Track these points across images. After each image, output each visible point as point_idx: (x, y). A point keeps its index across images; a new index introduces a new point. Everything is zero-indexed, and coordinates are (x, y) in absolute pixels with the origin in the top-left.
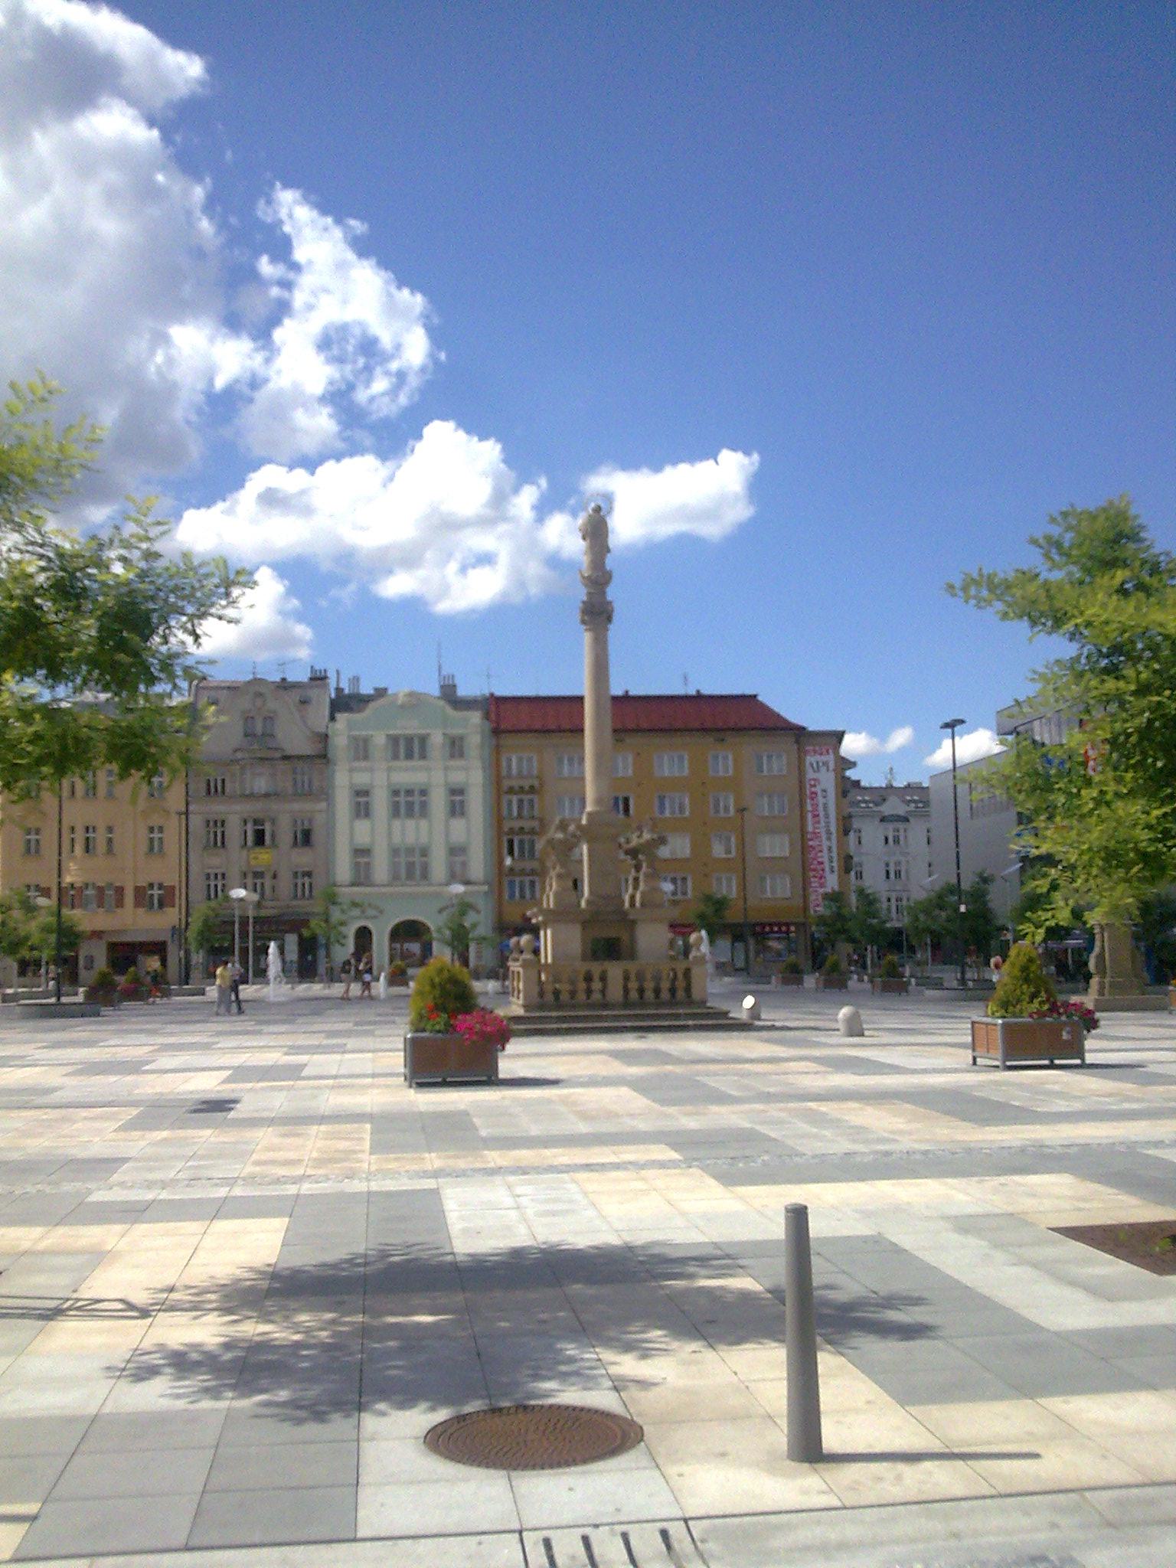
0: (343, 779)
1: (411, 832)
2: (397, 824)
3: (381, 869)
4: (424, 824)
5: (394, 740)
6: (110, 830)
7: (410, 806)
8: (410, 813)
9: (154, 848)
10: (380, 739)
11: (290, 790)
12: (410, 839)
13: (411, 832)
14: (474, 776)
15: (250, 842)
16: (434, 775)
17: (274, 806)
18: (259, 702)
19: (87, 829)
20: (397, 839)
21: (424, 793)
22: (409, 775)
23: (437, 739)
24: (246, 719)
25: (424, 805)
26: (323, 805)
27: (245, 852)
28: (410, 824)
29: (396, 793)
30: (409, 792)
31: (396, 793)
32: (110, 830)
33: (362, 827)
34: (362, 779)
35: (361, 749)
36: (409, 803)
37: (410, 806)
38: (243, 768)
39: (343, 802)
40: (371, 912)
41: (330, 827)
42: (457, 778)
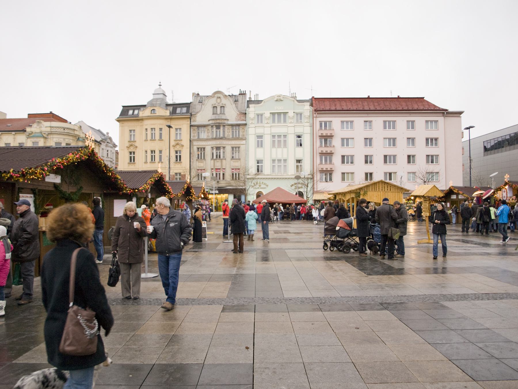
0: (252, 131)
1: (279, 153)
2: (274, 150)
3: (267, 169)
4: (285, 150)
5: (273, 114)
6: (161, 152)
7: (279, 142)
8: (279, 146)
9: (178, 159)
10: (267, 114)
11: (231, 137)
12: (279, 157)
13: (279, 153)
14: (305, 130)
15: (215, 157)
16: (290, 130)
17: (224, 142)
18: (219, 100)
19: (152, 151)
20: (274, 157)
21: (285, 136)
22: (279, 129)
23: (291, 114)
24: (214, 107)
25: (285, 141)
26: (244, 142)
27: (212, 161)
28: (280, 150)
29: (274, 136)
30: (279, 136)
31: (274, 136)
32: (161, 152)
33: (260, 150)
34: (260, 131)
35: (260, 116)
36: (279, 140)
37: (279, 142)
38: (212, 126)
39: (252, 140)
40: (263, 186)
41: (247, 150)
42: (299, 130)
